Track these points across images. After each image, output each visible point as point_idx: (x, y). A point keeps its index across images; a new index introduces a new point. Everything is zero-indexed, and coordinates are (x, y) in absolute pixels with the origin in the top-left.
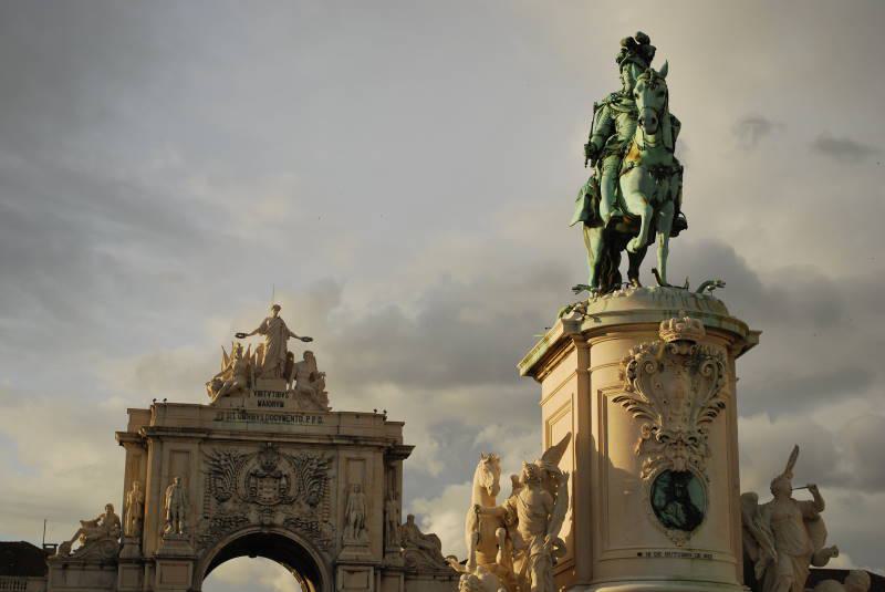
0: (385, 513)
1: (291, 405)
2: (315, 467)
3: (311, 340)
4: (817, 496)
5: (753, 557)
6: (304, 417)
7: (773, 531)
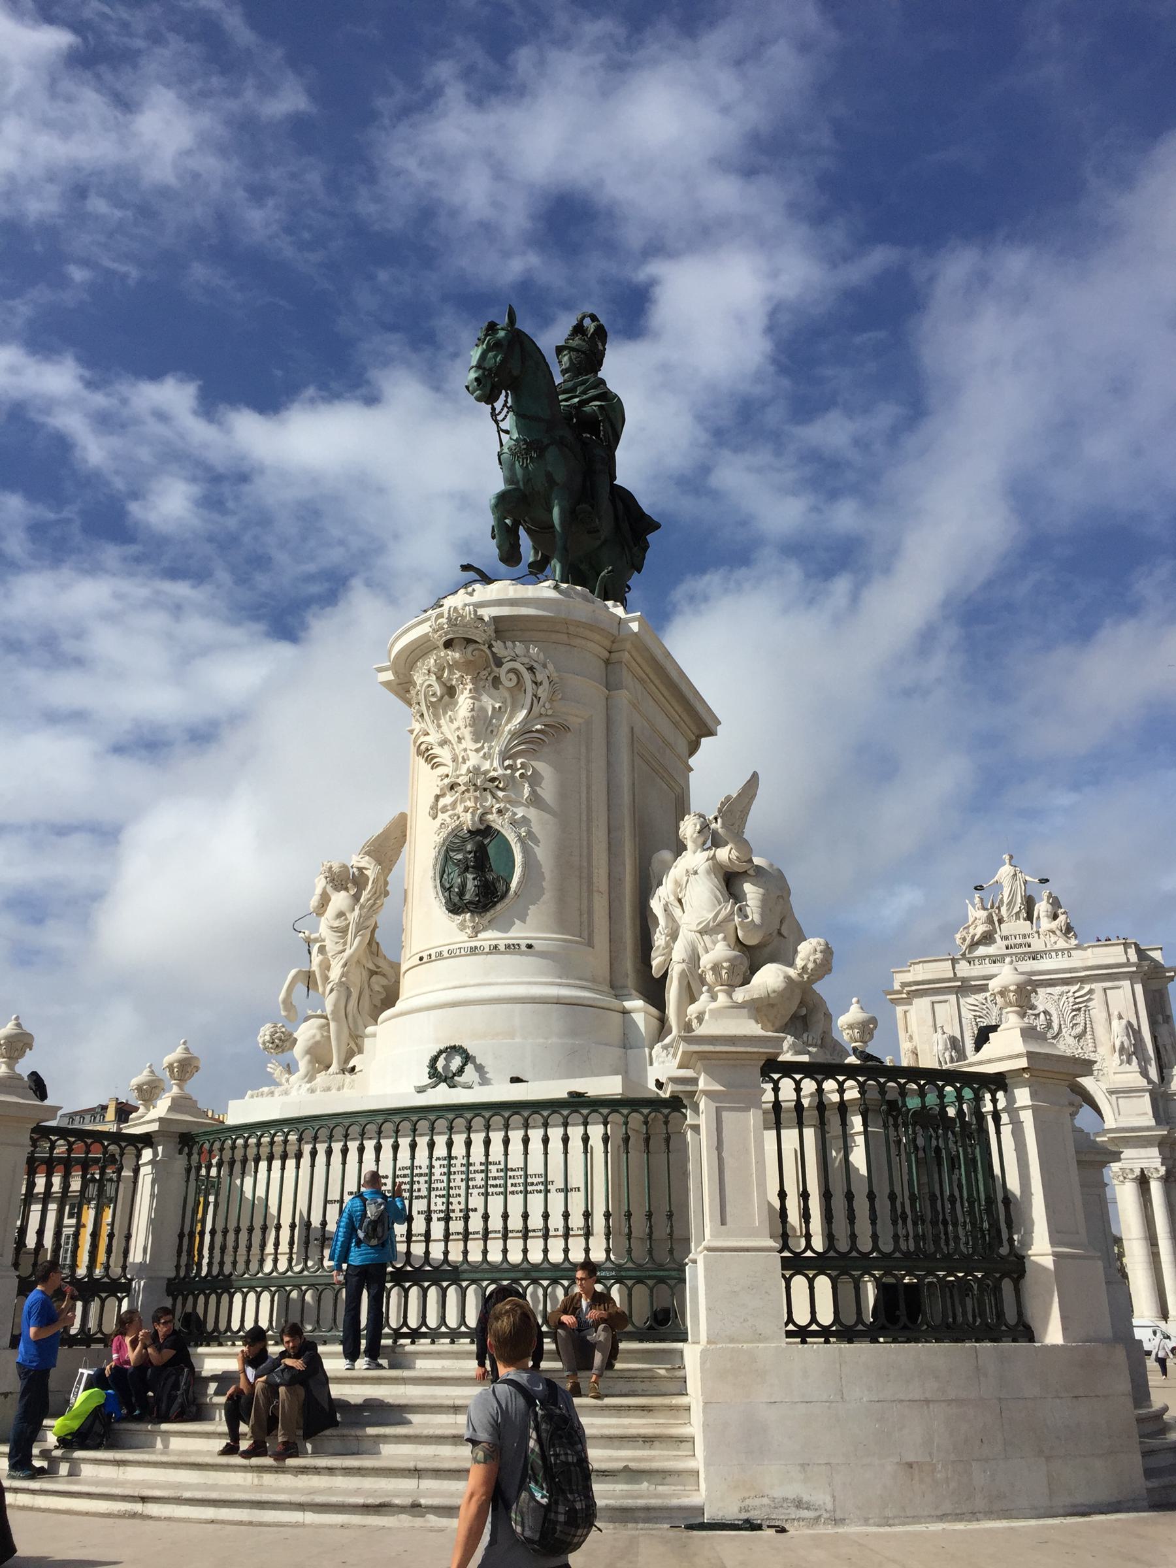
1: (1037, 945)
3: (1047, 881)
6: (1053, 954)
7: (680, 901)
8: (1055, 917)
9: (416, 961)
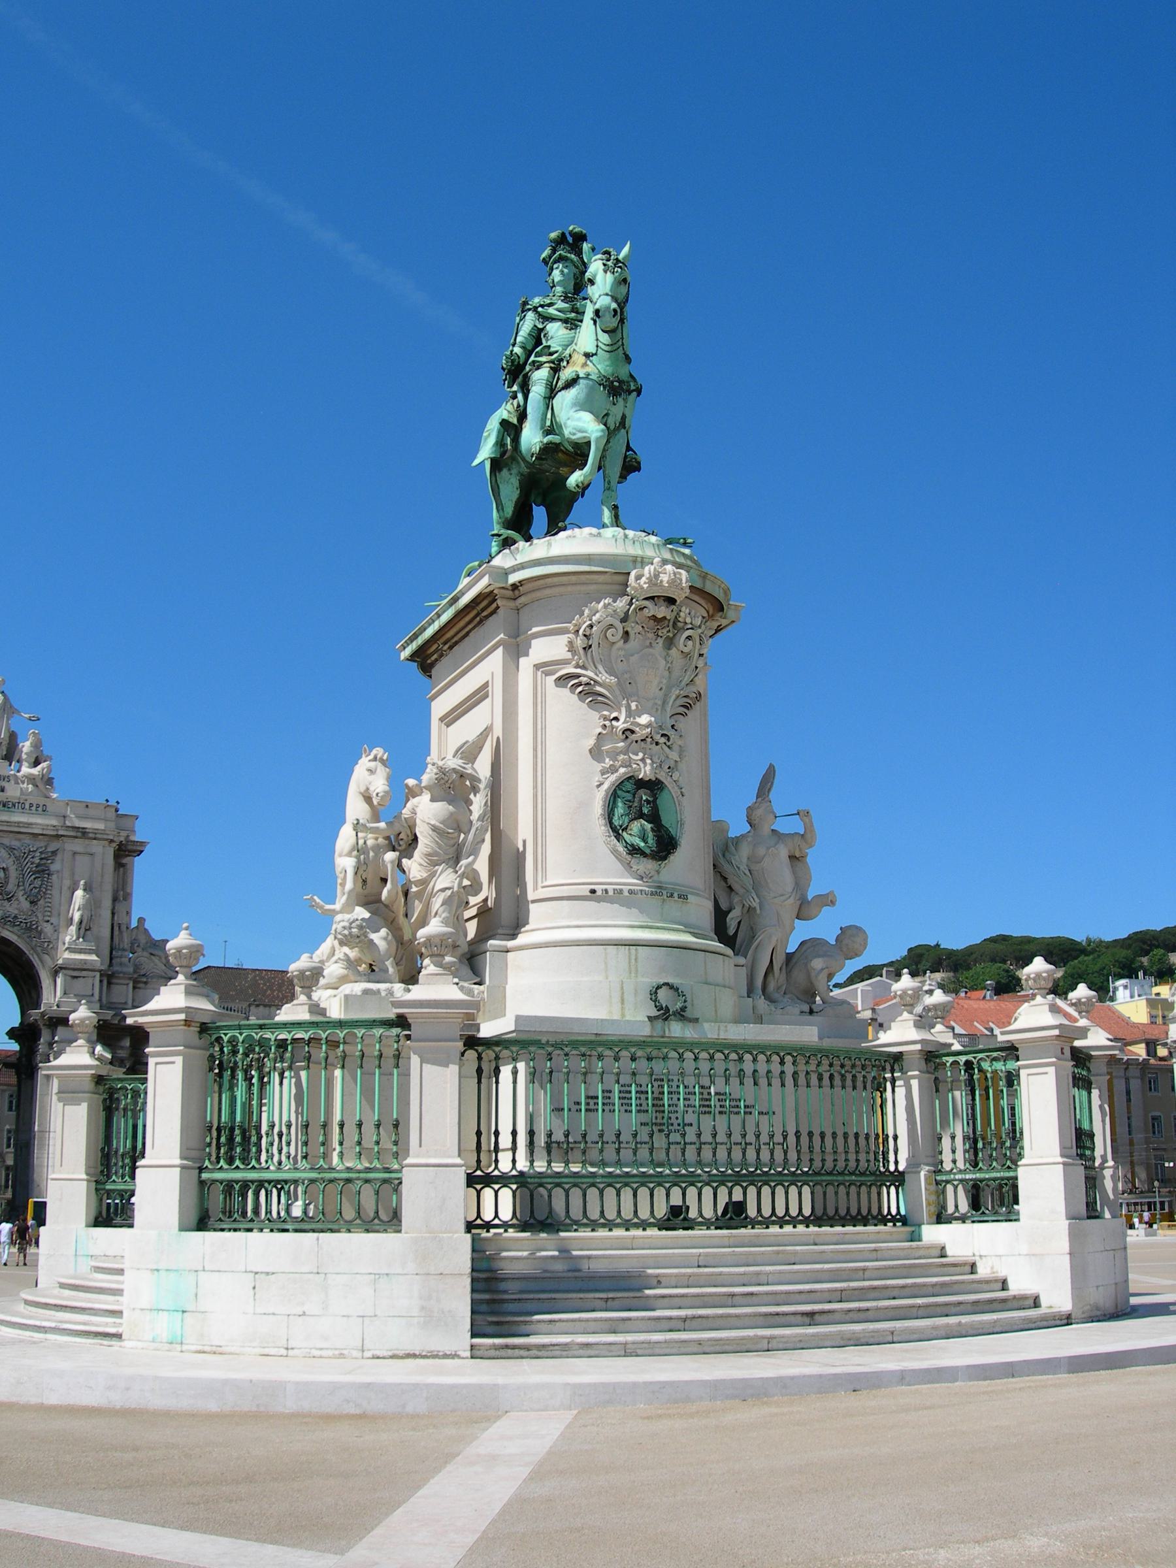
0: (113, 914)
2: (37, 861)
4: (809, 828)
5: (724, 906)
8: (36, 763)
9: (585, 890)
